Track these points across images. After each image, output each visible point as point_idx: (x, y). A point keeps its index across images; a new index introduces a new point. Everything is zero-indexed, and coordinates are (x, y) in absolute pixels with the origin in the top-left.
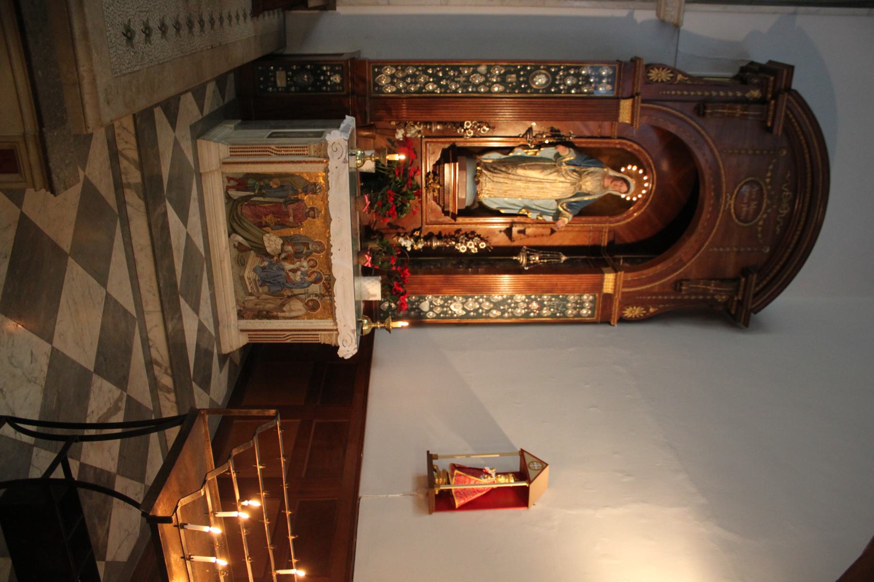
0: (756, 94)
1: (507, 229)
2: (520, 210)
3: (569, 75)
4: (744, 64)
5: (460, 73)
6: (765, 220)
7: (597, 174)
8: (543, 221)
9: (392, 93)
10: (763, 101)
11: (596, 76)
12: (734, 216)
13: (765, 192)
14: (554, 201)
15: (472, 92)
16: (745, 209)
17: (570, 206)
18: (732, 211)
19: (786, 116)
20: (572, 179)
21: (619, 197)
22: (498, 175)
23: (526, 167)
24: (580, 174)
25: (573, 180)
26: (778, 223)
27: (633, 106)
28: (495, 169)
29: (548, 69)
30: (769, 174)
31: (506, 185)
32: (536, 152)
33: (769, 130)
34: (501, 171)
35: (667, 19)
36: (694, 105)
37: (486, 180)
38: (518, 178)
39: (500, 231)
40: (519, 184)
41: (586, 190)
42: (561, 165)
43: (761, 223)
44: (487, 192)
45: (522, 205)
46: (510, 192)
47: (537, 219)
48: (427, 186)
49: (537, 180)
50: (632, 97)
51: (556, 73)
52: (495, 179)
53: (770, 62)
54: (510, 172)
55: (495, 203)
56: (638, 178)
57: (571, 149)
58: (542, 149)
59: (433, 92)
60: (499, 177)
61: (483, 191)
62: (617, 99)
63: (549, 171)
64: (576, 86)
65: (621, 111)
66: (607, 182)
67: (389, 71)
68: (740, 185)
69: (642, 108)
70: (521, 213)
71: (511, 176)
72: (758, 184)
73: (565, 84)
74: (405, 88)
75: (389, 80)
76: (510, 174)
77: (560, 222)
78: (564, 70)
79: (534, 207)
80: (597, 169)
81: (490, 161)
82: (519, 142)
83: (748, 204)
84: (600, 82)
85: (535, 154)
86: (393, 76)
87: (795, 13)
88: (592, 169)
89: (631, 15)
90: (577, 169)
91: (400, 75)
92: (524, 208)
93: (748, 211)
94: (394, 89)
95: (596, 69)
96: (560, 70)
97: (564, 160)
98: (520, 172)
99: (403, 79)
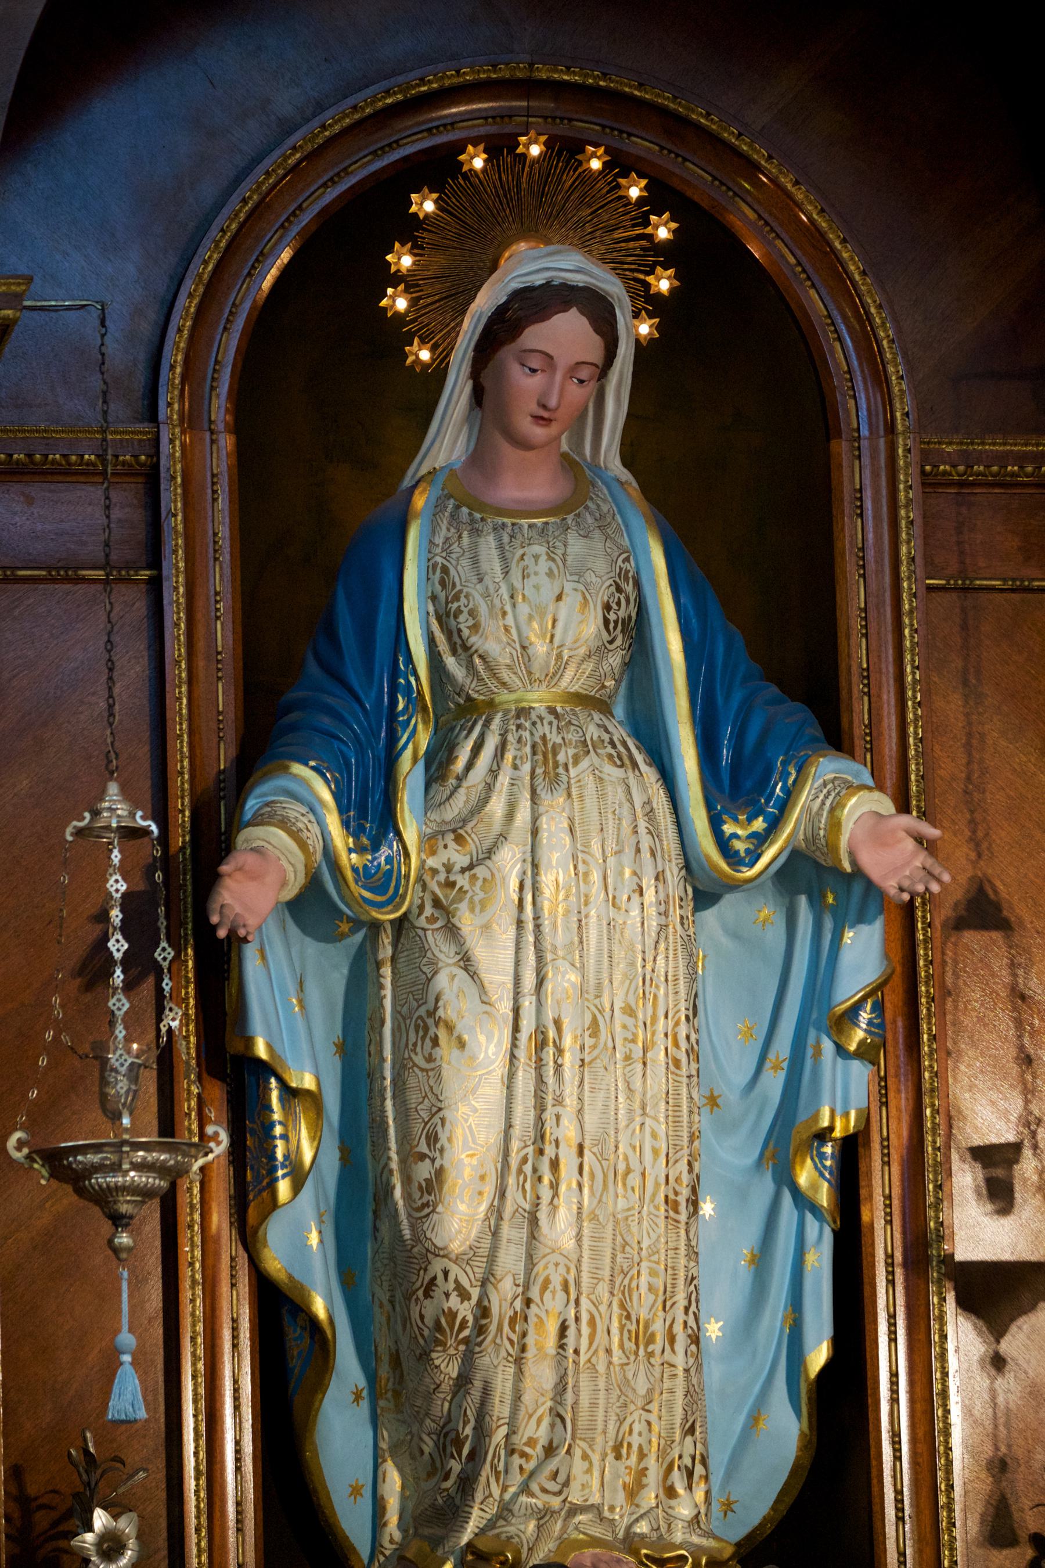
1: (965, 1304)
2: (803, 1202)
7: (461, 571)
8: (894, 999)
14: (710, 915)
20: (504, 779)
21: (642, 350)
22: (500, 1409)
23: (423, 1171)
31: (579, 1338)
32: (289, 1093)
34: (463, 1381)
37: (544, 1515)
38: (512, 1233)
39: (998, 1362)
41: (600, 652)
44: (649, 1497)
45: (766, 1185)
46: (644, 1305)
47: (864, 1053)
49: (524, 1079)
54: (465, 1311)
55: (754, 1419)
57: (252, 804)
58: (261, 1050)
60: (517, 1397)
61: (643, 1528)
70: (824, 1196)
76: (483, 1311)
77: (874, 864)
79: (774, 1083)
81: (393, 1481)
82: (209, 1244)
85: (313, 1100)
92: (785, 1179)
97: (350, 860)
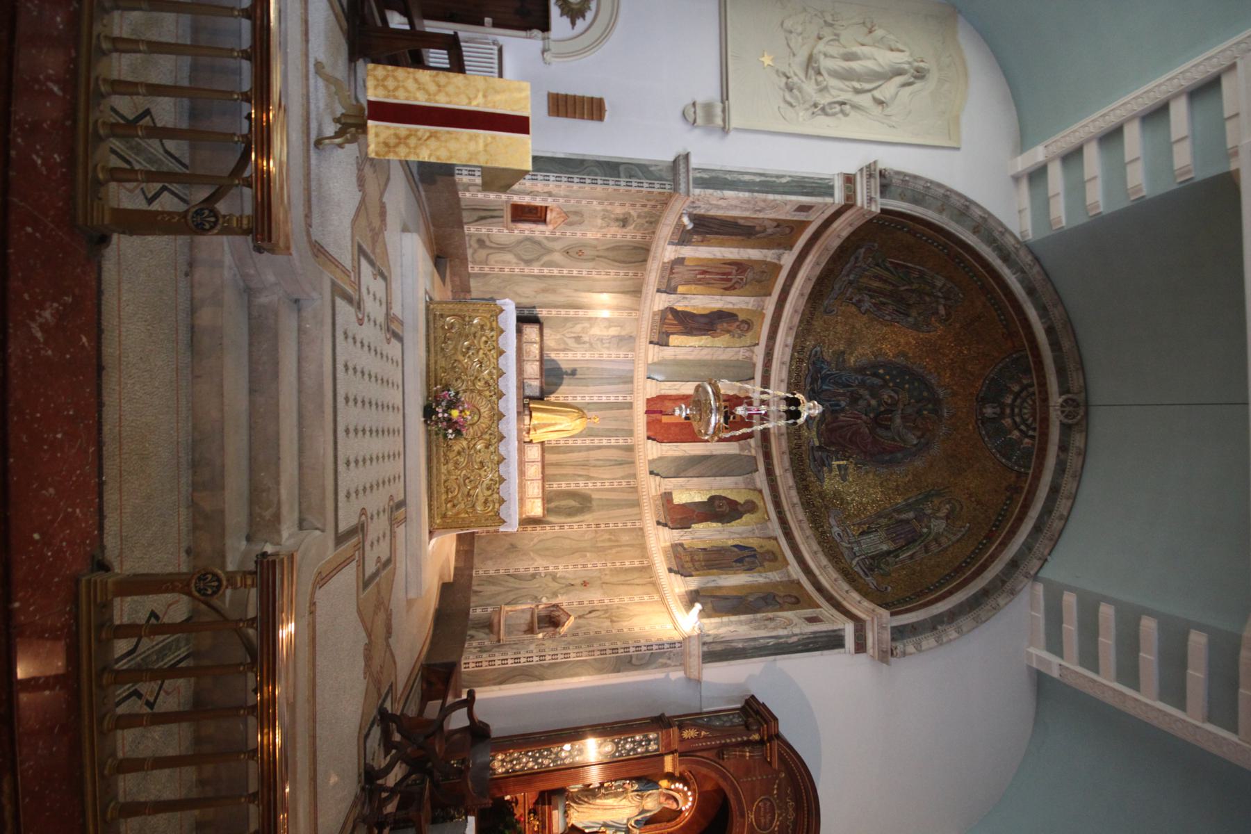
0: (756, 737)
3: (627, 742)
4: (747, 698)
5: (551, 752)
6: (779, 826)
9: (503, 773)
10: (761, 742)
11: (646, 741)
12: (756, 827)
13: (775, 805)
15: (560, 765)
16: (763, 821)
17: (637, 822)
18: (754, 823)
19: (779, 752)
24: (642, 797)
25: (638, 804)
26: (788, 826)
27: (673, 760)
28: (580, 799)
29: (613, 741)
30: (775, 792)
33: (770, 763)
35: (692, 677)
36: (716, 751)
40: (599, 812)
42: (627, 793)
43: (776, 829)
48: (528, 823)
50: (672, 753)
51: (619, 743)
52: (580, 810)
53: (764, 705)
56: (685, 794)
59: (532, 768)
62: (662, 755)
63: (620, 798)
64: (634, 749)
65: (666, 764)
66: (662, 799)
67: (500, 757)
68: (756, 803)
69: (680, 760)
71: (592, 806)
72: (770, 800)
73: (625, 749)
74: (512, 768)
75: (500, 763)
78: (624, 739)
79: (611, 823)
80: (654, 791)
81: (576, 790)
83: (765, 817)
84: (649, 744)
86: (503, 761)
87: (775, 660)
88: (651, 792)
89: (667, 676)
90: (640, 793)
91: (508, 759)
93: (765, 822)
94: (504, 770)
95: (646, 736)
96: (621, 740)
98: (598, 801)
99: (511, 761)
